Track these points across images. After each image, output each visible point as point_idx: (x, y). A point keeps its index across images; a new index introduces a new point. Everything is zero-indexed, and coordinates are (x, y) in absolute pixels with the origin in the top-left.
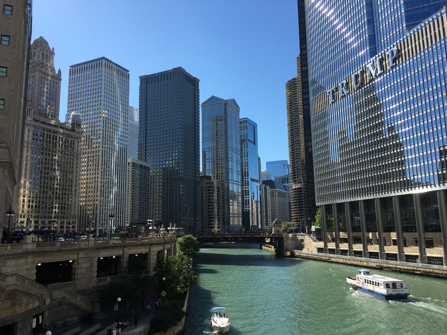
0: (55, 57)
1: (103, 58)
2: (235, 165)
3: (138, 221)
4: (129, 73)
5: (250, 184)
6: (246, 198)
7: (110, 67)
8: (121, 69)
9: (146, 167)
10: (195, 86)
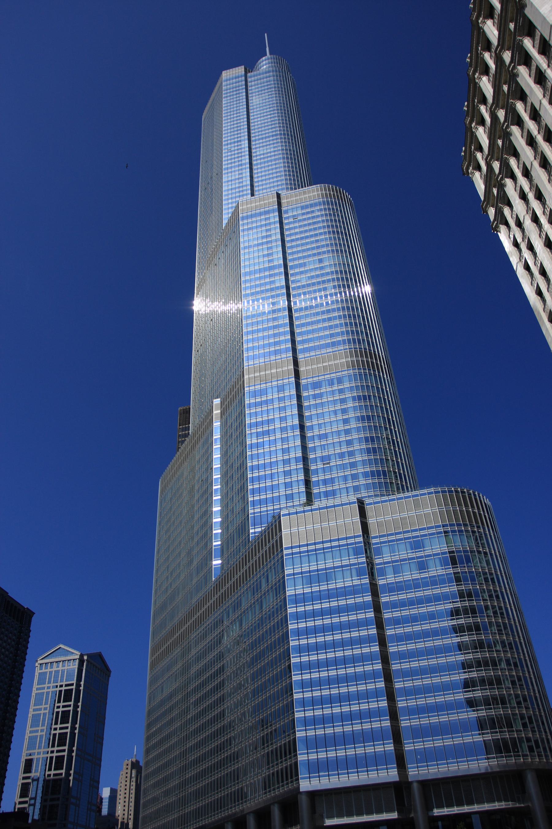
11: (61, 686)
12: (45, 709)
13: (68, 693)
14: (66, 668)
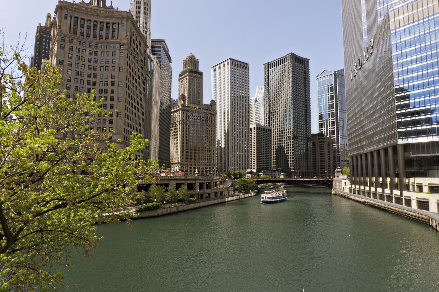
0: (199, 64)
3: (263, 168)
4: (249, 65)
8: (242, 64)
9: (268, 130)
10: (304, 65)
11: (328, 86)
12: (323, 96)
13: (332, 89)
14: (329, 78)
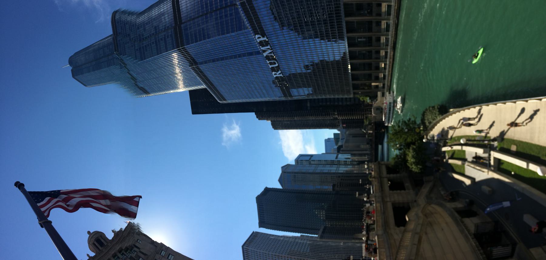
1: (243, 246)
2: (326, 168)
5: (339, 160)
6: (348, 163)
7: (249, 244)
8: (252, 237)
